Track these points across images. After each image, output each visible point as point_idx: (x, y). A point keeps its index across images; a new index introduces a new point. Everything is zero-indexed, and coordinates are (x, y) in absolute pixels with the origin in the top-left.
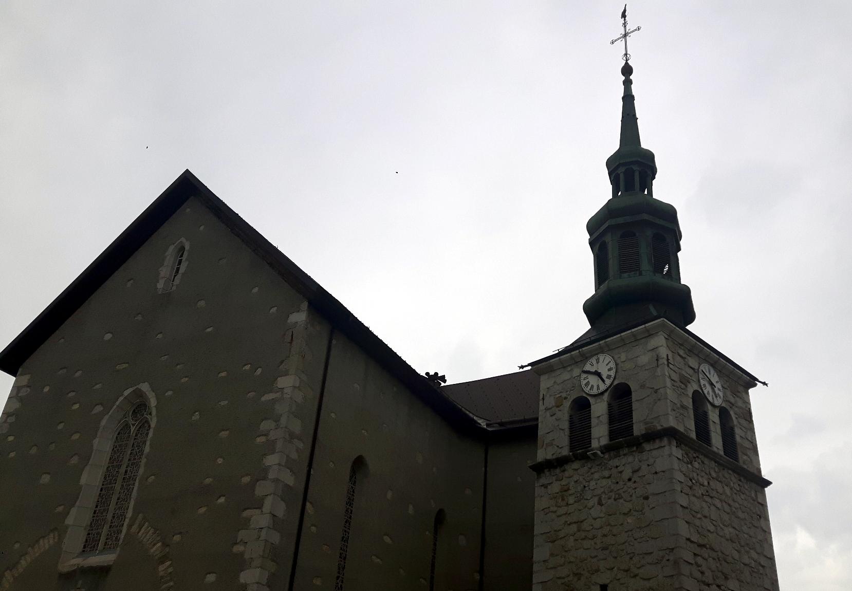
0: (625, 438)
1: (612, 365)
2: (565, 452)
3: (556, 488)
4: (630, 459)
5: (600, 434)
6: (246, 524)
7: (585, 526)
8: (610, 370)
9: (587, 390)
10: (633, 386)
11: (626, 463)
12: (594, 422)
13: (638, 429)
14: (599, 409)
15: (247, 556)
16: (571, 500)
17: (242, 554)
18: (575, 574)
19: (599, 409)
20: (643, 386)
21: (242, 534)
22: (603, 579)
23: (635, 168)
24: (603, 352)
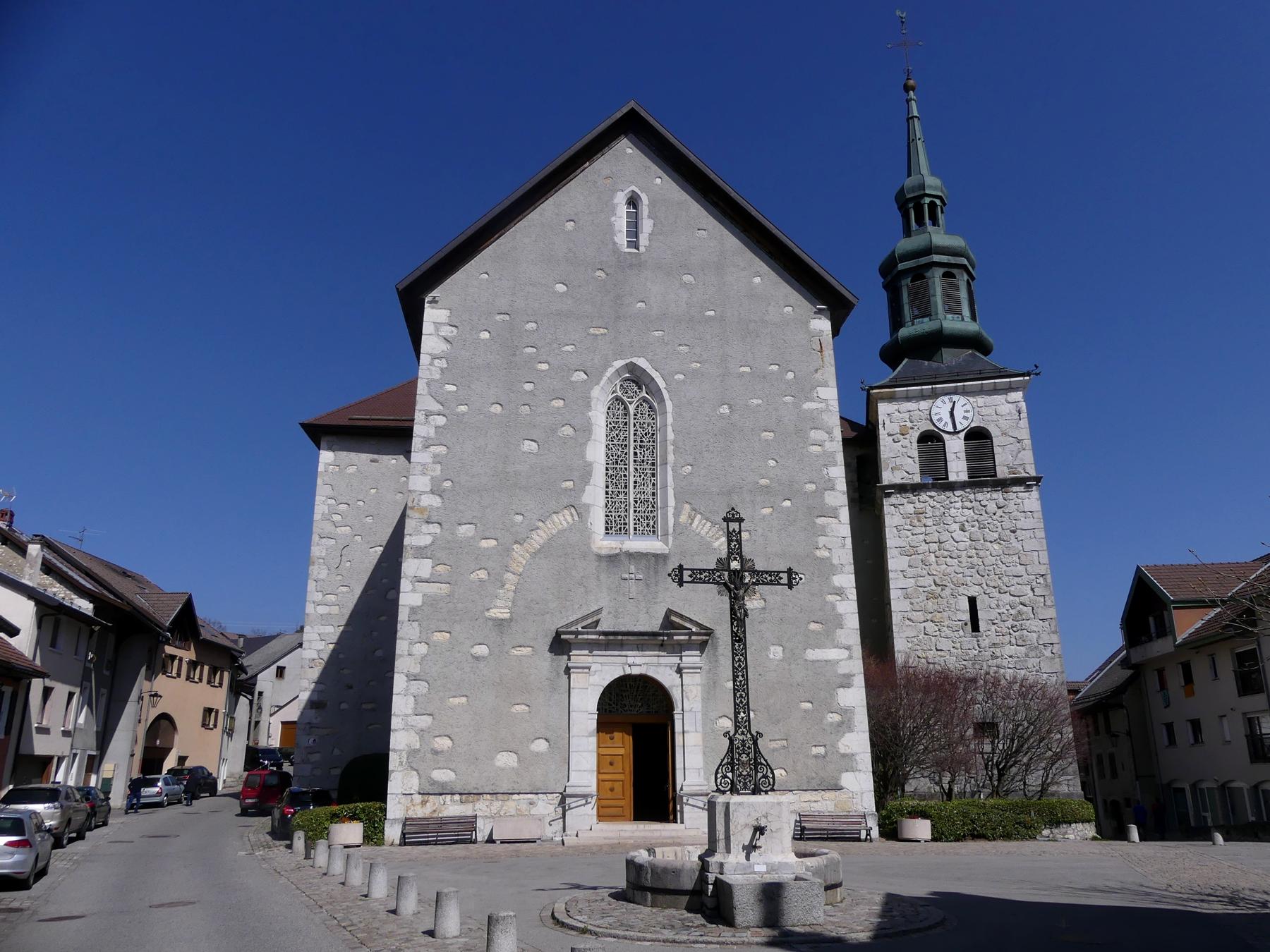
0: (984, 476)
1: (968, 407)
2: (917, 479)
3: (910, 508)
4: (995, 495)
5: (958, 469)
6: (823, 531)
7: (947, 546)
8: (967, 411)
9: (940, 425)
10: (994, 431)
11: (989, 498)
12: (950, 456)
13: (1002, 472)
14: (955, 447)
15: (835, 561)
16: (929, 522)
17: (829, 559)
18: (936, 585)
19: (955, 447)
20: (1004, 434)
21: (822, 540)
22: (973, 591)
23: (938, 202)
24: (956, 393)
